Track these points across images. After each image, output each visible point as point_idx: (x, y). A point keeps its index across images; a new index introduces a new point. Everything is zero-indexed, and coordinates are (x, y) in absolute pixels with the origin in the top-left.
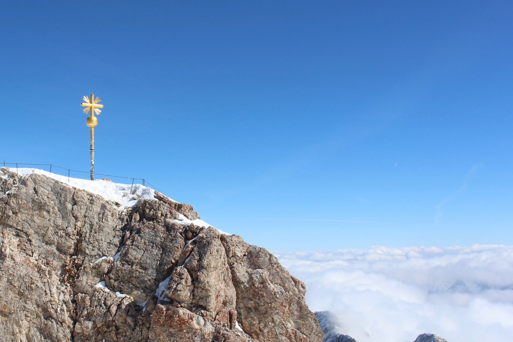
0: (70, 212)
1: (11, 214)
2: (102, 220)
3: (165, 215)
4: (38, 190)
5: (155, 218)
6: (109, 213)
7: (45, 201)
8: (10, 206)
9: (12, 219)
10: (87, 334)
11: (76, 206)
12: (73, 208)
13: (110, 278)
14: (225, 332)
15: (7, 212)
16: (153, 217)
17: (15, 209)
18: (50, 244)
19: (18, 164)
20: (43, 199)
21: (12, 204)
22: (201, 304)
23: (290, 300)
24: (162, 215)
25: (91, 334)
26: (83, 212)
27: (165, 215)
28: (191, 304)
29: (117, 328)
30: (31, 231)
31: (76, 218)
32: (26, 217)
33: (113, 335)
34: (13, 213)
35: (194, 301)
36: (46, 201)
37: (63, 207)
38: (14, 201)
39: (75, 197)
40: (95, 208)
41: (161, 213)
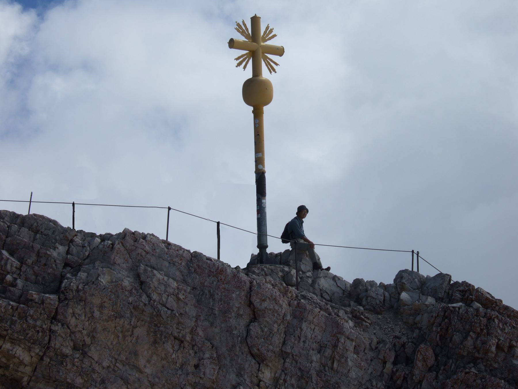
0: (241, 343)
1: (68, 351)
2: (333, 363)
3: (506, 350)
4: (148, 280)
5: (482, 359)
6: (348, 343)
8: (66, 326)
9: (74, 365)
11: (256, 324)
15: (57, 343)
16: (477, 355)
17: (82, 333)
19: (75, 205)
20: (164, 306)
21: (73, 321)
24: (499, 347)
26: (277, 340)
27: (506, 350)
32: (113, 357)
34: (75, 348)
36: (172, 311)
37: (221, 328)
38: (80, 313)
40: (309, 330)
41: (497, 343)
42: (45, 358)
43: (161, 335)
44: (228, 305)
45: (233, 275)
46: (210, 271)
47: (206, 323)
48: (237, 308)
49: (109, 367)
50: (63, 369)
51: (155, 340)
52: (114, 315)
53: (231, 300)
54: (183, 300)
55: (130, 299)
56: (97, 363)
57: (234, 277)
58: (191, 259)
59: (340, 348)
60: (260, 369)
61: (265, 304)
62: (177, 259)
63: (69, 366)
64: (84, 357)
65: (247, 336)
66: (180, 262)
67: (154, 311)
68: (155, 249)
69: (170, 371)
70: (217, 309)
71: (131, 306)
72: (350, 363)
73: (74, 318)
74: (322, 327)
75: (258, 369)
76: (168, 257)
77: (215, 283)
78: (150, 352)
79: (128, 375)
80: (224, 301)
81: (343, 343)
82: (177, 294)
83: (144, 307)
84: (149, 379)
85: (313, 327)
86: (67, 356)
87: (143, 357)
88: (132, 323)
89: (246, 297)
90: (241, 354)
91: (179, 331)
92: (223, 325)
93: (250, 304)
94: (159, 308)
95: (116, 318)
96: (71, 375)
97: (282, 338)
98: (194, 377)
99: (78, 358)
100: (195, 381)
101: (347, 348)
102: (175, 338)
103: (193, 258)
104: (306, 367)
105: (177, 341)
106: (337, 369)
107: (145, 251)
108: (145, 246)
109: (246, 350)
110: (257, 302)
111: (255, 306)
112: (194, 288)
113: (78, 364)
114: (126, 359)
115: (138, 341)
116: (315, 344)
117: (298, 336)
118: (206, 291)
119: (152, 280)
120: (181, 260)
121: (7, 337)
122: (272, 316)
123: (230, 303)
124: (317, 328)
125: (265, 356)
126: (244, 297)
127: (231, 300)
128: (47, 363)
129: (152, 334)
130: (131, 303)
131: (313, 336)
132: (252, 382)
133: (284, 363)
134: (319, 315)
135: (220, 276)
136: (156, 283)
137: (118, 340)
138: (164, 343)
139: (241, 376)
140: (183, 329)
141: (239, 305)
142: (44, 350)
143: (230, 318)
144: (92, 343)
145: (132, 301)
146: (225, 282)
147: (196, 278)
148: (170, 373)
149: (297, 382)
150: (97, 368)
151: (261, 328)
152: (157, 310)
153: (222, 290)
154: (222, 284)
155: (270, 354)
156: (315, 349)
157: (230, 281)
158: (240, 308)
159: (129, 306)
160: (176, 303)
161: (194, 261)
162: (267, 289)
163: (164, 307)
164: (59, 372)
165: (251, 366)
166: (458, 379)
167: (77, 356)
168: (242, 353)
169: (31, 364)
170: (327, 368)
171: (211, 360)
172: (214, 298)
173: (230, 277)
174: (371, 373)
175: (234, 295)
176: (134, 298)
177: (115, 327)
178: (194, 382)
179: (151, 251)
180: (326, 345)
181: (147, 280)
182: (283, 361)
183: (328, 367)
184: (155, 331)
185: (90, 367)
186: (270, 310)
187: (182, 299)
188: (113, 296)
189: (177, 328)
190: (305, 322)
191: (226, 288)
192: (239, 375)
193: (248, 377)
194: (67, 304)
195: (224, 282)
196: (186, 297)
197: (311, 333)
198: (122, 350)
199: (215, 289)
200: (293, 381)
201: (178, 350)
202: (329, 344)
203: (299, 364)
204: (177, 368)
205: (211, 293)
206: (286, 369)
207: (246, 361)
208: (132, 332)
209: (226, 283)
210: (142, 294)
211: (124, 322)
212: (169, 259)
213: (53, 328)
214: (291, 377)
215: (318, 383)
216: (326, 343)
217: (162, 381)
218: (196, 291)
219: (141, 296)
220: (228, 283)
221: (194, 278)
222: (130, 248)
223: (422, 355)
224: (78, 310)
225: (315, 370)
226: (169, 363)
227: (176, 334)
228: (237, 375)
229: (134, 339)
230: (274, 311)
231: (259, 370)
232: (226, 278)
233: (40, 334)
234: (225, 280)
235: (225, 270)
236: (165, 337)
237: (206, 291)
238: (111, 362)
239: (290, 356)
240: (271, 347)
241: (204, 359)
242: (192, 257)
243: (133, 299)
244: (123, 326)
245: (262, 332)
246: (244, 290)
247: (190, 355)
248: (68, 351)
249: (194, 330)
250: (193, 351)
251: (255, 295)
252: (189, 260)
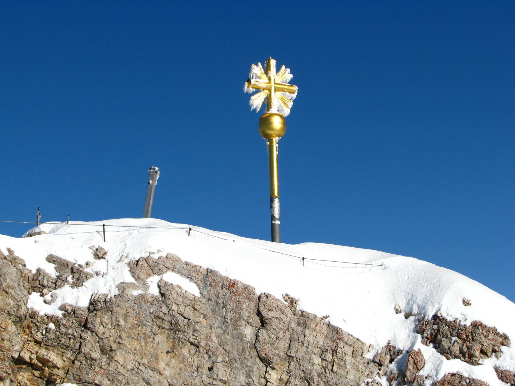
0: (250, 348)
1: (96, 354)
2: (333, 366)
6: (347, 348)
7: (186, 321)
8: (94, 334)
9: (101, 368)
12: (257, 336)
15: (86, 349)
21: (101, 329)
26: (283, 345)
31: (266, 362)
32: (137, 361)
36: (189, 319)
38: (107, 322)
39: (262, 309)
40: (312, 336)
41: (481, 348)
42: (76, 362)
43: (179, 341)
44: (239, 314)
45: (243, 288)
46: (223, 284)
47: (220, 331)
48: (247, 318)
49: (133, 369)
50: (92, 371)
51: (174, 346)
52: (137, 323)
53: (241, 310)
54: (199, 310)
55: (152, 310)
56: (122, 366)
57: (245, 289)
58: (207, 274)
59: (339, 352)
60: (267, 371)
61: (272, 314)
62: (194, 274)
63: (97, 369)
64: (111, 361)
65: (256, 342)
66: (197, 277)
67: (172, 320)
68: (174, 266)
69: (187, 373)
70: (229, 318)
71: (153, 316)
72: (348, 366)
73: (102, 327)
74: (324, 334)
75: (265, 371)
76: (186, 272)
77: (228, 295)
78: (169, 357)
79: (149, 377)
80: (235, 311)
81: (342, 348)
82: (193, 305)
83: (164, 317)
84: (168, 381)
85: (315, 333)
86: (95, 360)
87: (162, 360)
88: (153, 331)
89: (256, 307)
90: (250, 358)
91: (195, 337)
92: (234, 332)
93: (259, 314)
94: (177, 318)
95: (139, 326)
96: (99, 377)
97: (288, 343)
98: (208, 379)
99: (105, 362)
100: (209, 382)
101: (346, 352)
102: (192, 344)
103: (208, 273)
104: (309, 369)
105: (193, 347)
106: (336, 371)
107: (166, 267)
108: (166, 263)
109: (255, 353)
110: (264, 312)
111: (263, 315)
112: (209, 300)
113: (105, 367)
114: (148, 362)
115: (158, 347)
116: (317, 349)
117: (302, 341)
118: (220, 302)
119: (171, 293)
120: (198, 275)
121: (42, 344)
122: (278, 324)
123: (240, 312)
124: (319, 335)
125: (271, 360)
126: (253, 308)
127: (241, 310)
128: (78, 367)
129: (171, 340)
130: (152, 313)
131: (315, 342)
132: (260, 383)
133: (289, 366)
134: (320, 323)
135: (232, 288)
136: (175, 296)
137: (141, 345)
138: (181, 348)
139: (250, 377)
140: (198, 336)
141: (249, 315)
142: (75, 355)
143: (241, 326)
144: (117, 349)
145: (153, 311)
146: (237, 294)
147: (211, 291)
148: (187, 375)
149: (300, 382)
150: (122, 370)
151: (268, 335)
152: (175, 319)
153: (234, 301)
154: (233, 296)
155: (276, 358)
156: (317, 353)
157: (240, 293)
158: (250, 317)
159: (150, 316)
160: (193, 313)
161: (210, 276)
162: (274, 301)
163: (182, 317)
164: (88, 374)
165: (259, 369)
166: (445, 381)
167: (105, 360)
168: (251, 357)
169: (64, 368)
170: (327, 371)
171: (223, 363)
172: (226, 308)
173: (241, 289)
174: (368, 375)
175: (244, 306)
176: (155, 308)
177: (138, 334)
178: (208, 382)
179: (171, 267)
180: (327, 350)
181: (167, 292)
182: (288, 364)
183: (328, 369)
184: (174, 338)
185: (116, 370)
186: (277, 318)
187: (198, 309)
188: (136, 307)
189: (193, 335)
190: (308, 329)
191: (238, 299)
192: (248, 376)
193: (256, 378)
194: (96, 314)
195: (235, 294)
196: (201, 308)
197: (313, 339)
198: (144, 355)
199: (228, 300)
201: (194, 354)
202: (329, 349)
203: (302, 367)
204: (193, 370)
205: (224, 304)
206: (290, 371)
207: (255, 364)
208: (154, 338)
209: (237, 295)
210: (162, 305)
211: (146, 330)
212: (187, 274)
213: (83, 335)
214: (295, 378)
215: (319, 383)
216: (327, 348)
217: (180, 382)
218: (211, 302)
219: (160, 307)
220: (239, 295)
221: (209, 290)
222: (153, 264)
223: (413, 359)
224: (106, 319)
225: (317, 372)
226: (186, 366)
227: (192, 340)
228: (247, 377)
229: (155, 345)
230: (280, 319)
231: (266, 372)
232: (237, 290)
233: (72, 340)
234: (236, 292)
235: (237, 284)
236: (183, 343)
237: (220, 302)
238: (135, 365)
239: (295, 359)
240: (277, 352)
241: (217, 362)
242: (208, 272)
243: (154, 309)
244: (145, 334)
245: (269, 338)
246: (253, 301)
247: (205, 359)
248: (97, 356)
249: (209, 336)
250: (207, 355)
251: (263, 305)
252: (206, 275)
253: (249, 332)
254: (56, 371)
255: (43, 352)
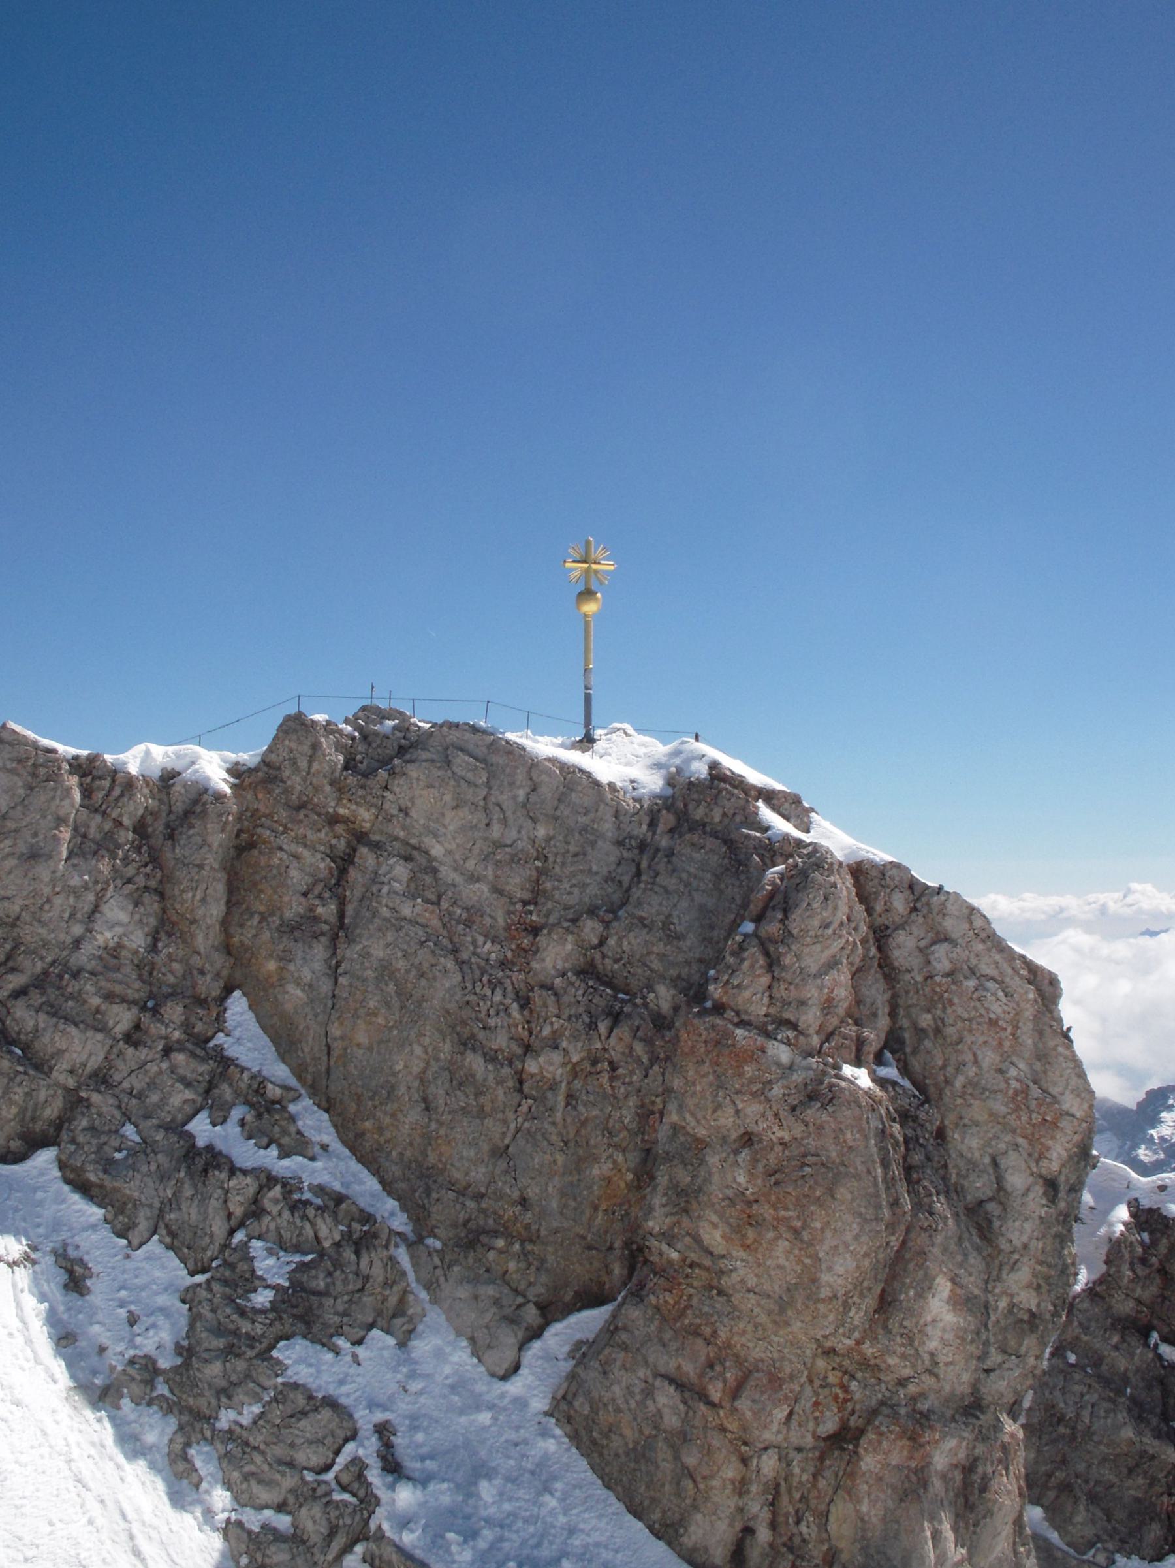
1: (394, 812)
10: (549, 1076)
13: (604, 956)
14: (835, 1080)
15: (386, 806)
18: (478, 880)
21: (397, 790)
22: (787, 1015)
23: (1017, 1014)
25: (558, 1078)
28: (766, 1016)
29: (613, 1067)
30: (437, 851)
31: (534, 820)
33: (605, 1079)
34: (401, 810)
35: (772, 1010)
192: (519, 832)
200: (561, 838)
253: (521, 794)
254: (364, 824)
255: (354, 807)
